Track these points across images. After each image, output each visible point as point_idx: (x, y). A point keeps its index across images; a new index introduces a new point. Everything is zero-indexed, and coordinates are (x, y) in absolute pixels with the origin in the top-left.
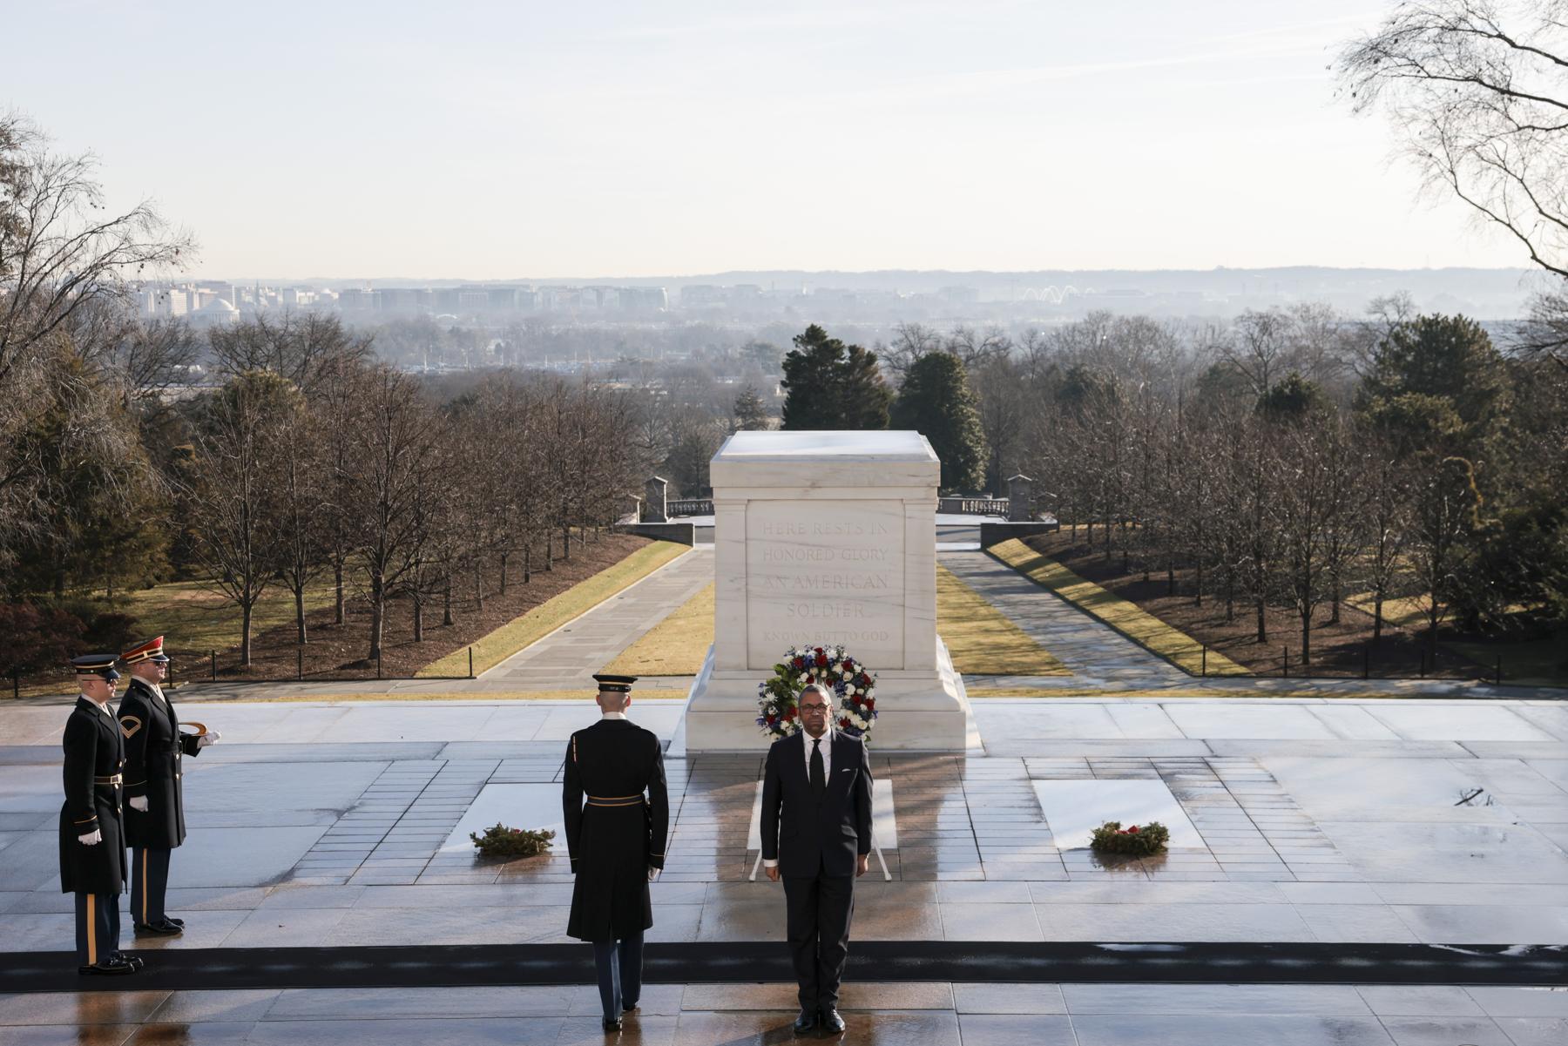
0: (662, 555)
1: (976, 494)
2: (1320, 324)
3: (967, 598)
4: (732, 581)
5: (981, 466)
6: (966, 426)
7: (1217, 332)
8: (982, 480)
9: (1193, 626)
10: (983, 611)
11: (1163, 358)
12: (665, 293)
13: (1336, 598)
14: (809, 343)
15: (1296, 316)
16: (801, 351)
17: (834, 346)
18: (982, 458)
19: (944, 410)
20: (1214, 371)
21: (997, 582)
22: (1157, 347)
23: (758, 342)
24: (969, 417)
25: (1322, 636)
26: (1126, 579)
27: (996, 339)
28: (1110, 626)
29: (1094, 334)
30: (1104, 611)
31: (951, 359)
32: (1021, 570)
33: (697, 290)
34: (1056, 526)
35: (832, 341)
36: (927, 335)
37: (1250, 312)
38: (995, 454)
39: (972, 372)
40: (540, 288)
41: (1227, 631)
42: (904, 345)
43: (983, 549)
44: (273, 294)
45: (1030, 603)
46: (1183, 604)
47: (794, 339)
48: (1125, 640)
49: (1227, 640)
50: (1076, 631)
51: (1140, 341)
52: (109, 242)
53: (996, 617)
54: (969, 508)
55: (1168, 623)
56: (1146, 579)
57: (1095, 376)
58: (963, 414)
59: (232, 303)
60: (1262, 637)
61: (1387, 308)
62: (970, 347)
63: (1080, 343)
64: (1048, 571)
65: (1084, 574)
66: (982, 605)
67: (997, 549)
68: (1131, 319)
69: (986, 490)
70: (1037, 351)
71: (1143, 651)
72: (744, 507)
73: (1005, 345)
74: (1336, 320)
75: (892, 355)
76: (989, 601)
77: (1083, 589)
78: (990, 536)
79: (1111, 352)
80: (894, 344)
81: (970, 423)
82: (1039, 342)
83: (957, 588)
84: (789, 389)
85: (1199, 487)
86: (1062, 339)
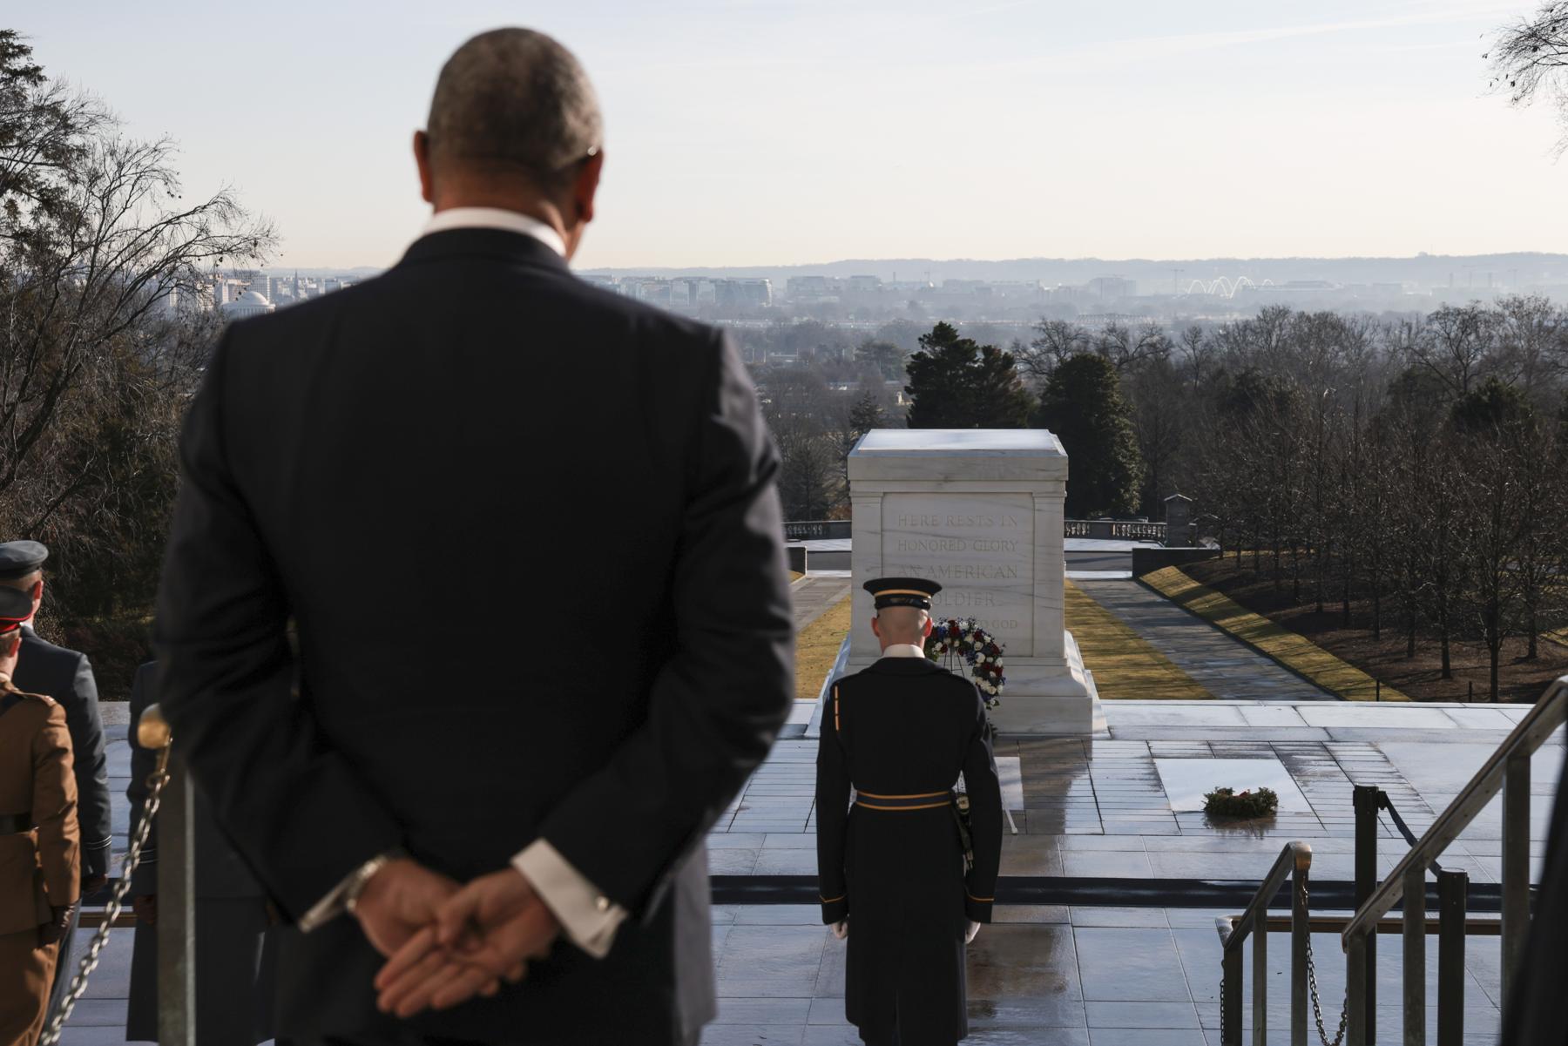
1: (1127, 516)
2: (1535, 321)
4: (867, 570)
6: (1118, 439)
7: (1413, 332)
8: (1136, 502)
9: (1370, 661)
10: (1133, 644)
11: (1350, 361)
12: (769, 285)
13: (1532, 631)
14: (937, 344)
15: (1507, 313)
16: (928, 352)
17: (967, 346)
18: (1137, 476)
19: (1093, 421)
20: (1408, 376)
21: (1149, 614)
22: (1343, 348)
23: (877, 342)
24: (1122, 429)
25: (1517, 672)
26: (1298, 609)
27: (1156, 338)
28: (1276, 660)
29: (1270, 333)
30: (1270, 645)
31: (1100, 362)
32: (1177, 601)
33: (805, 281)
34: (1220, 552)
35: (964, 342)
37: (1447, 308)
38: (1151, 472)
40: (624, 279)
41: (1410, 666)
43: (1135, 578)
44: (314, 286)
45: (1187, 636)
46: (1359, 638)
47: (920, 339)
48: (1291, 676)
49: (1406, 676)
50: (1237, 666)
51: (1323, 341)
52: (184, 234)
53: (1148, 650)
54: (1120, 532)
55: (1343, 659)
56: (1320, 609)
57: (1269, 382)
58: (1114, 425)
59: (266, 297)
60: (1447, 672)
62: (1124, 348)
63: (1252, 343)
64: (1208, 602)
65: (1248, 605)
67: (1151, 578)
68: (1312, 315)
69: (1141, 513)
70: (1202, 352)
71: (1312, 687)
72: (880, 499)
74: (1555, 316)
75: (1034, 357)
77: (1247, 621)
78: (1142, 563)
79: (1289, 355)
80: (1035, 344)
81: (1122, 436)
82: (1205, 341)
83: (1104, 620)
84: (914, 396)
85: (1377, 506)
86: (1232, 340)
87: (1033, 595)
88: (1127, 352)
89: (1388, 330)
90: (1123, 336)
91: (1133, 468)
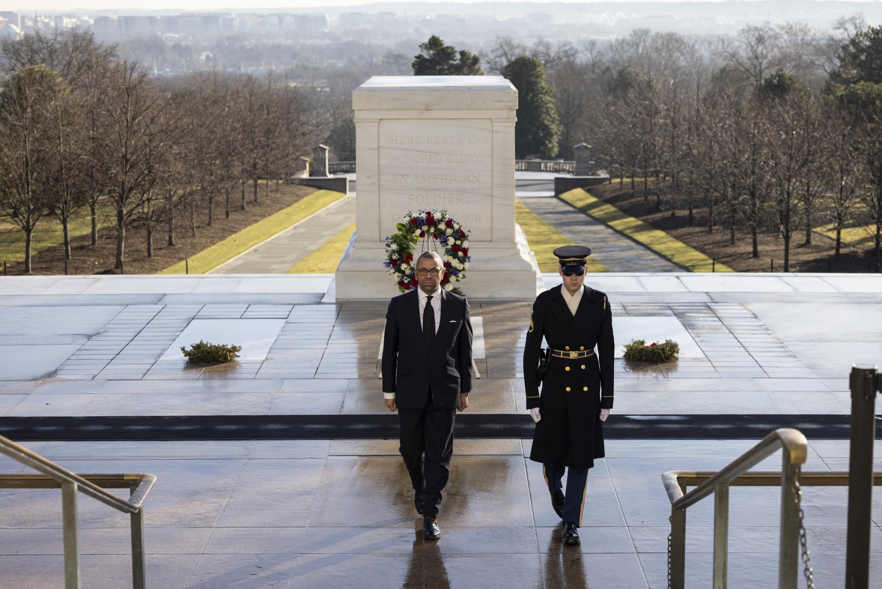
0: (324, 200)
1: (550, 158)
2: (800, 38)
3: (544, 229)
4: (368, 178)
5: (555, 139)
7: (726, 43)
9: (707, 247)
11: (687, 62)
12: (328, 18)
13: (808, 229)
14: (431, 48)
15: (782, 32)
17: (449, 50)
18: (556, 133)
19: (529, 98)
20: (723, 70)
22: (683, 54)
23: (395, 53)
24: (546, 103)
25: (798, 254)
26: (659, 215)
27: (567, 48)
28: (647, 247)
29: (638, 45)
30: (643, 237)
31: (533, 62)
32: (583, 210)
33: (350, 16)
34: (609, 179)
35: (448, 48)
36: (516, 45)
37: (749, 27)
38: (565, 131)
39: (550, 71)
41: (730, 250)
42: (499, 53)
45: (589, 232)
46: (699, 232)
47: (420, 46)
48: (656, 257)
49: (730, 256)
50: (622, 251)
51: (670, 50)
54: (546, 168)
55: (689, 245)
56: (673, 214)
57: (637, 75)
58: (542, 101)
60: (755, 254)
61: (847, 25)
62: (548, 54)
63: (627, 51)
64: (602, 210)
65: (629, 212)
66: (555, 233)
67: (566, 196)
68: (664, 34)
69: (559, 156)
70: (596, 57)
71: (670, 264)
73: (573, 53)
74: (812, 34)
75: (492, 60)
76: (560, 230)
77: (627, 223)
78: (561, 186)
79: (650, 59)
80: (493, 51)
81: (547, 108)
82: (598, 50)
83: (537, 222)
85: (711, 147)
86: (614, 49)
87: (492, 196)
88: (549, 56)
89: (710, 43)
90: (548, 46)
91: (554, 128)
